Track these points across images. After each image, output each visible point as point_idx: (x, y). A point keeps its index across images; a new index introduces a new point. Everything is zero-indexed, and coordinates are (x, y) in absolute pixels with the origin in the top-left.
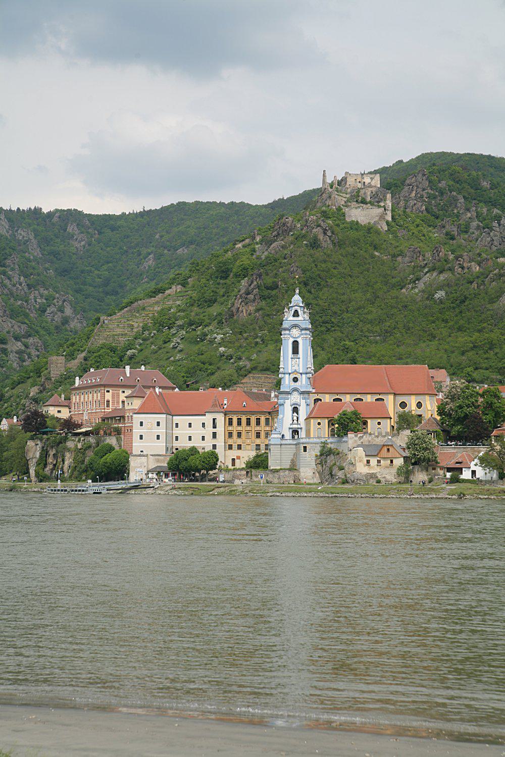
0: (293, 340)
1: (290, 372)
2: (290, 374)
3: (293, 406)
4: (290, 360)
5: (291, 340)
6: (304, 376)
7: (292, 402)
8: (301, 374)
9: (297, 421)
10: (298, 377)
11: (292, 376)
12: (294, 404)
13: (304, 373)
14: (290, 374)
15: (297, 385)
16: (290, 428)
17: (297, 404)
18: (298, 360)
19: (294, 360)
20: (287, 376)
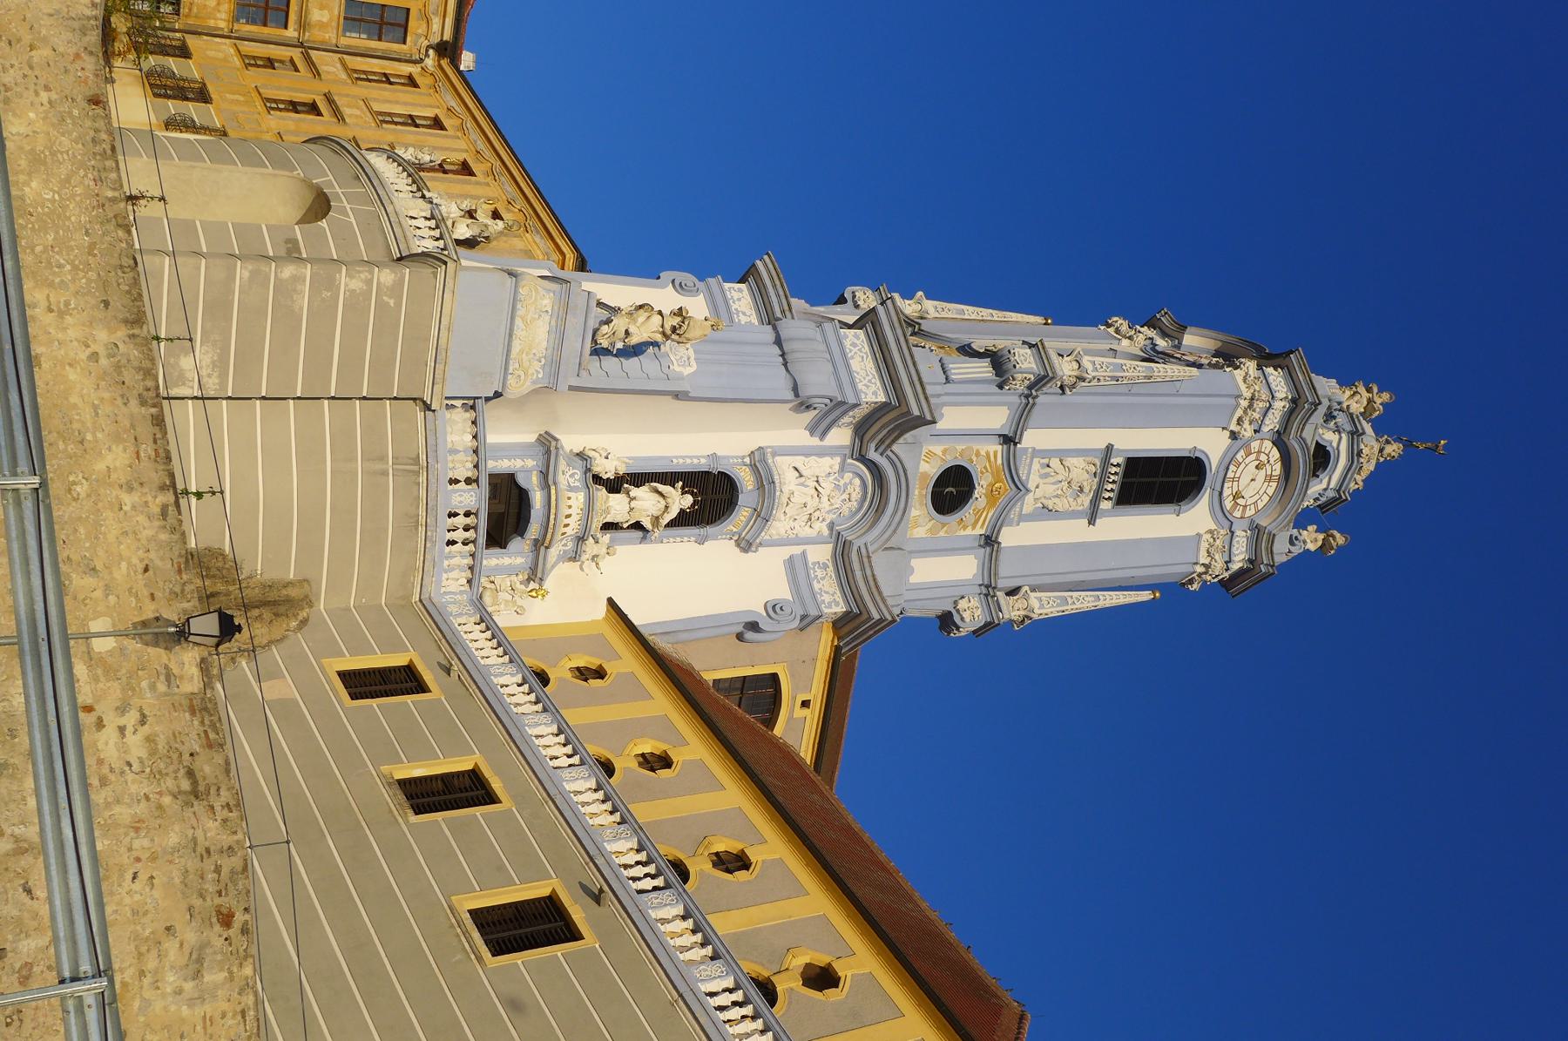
0: (1214, 460)
1: (1032, 439)
2: (1009, 440)
3: (745, 480)
4: (1097, 439)
5: (1209, 443)
6: (965, 568)
7: (783, 468)
8: (990, 541)
9: (608, 527)
10: (968, 512)
11: (984, 459)
12: (766, 483)
13: (991, 566)
14: (1009, 440)
15: (920, 518)
16: (547, 445)
17: (762, 516)
18: (1085, 500)
19: (1081, 471)
20: (997, 417)
